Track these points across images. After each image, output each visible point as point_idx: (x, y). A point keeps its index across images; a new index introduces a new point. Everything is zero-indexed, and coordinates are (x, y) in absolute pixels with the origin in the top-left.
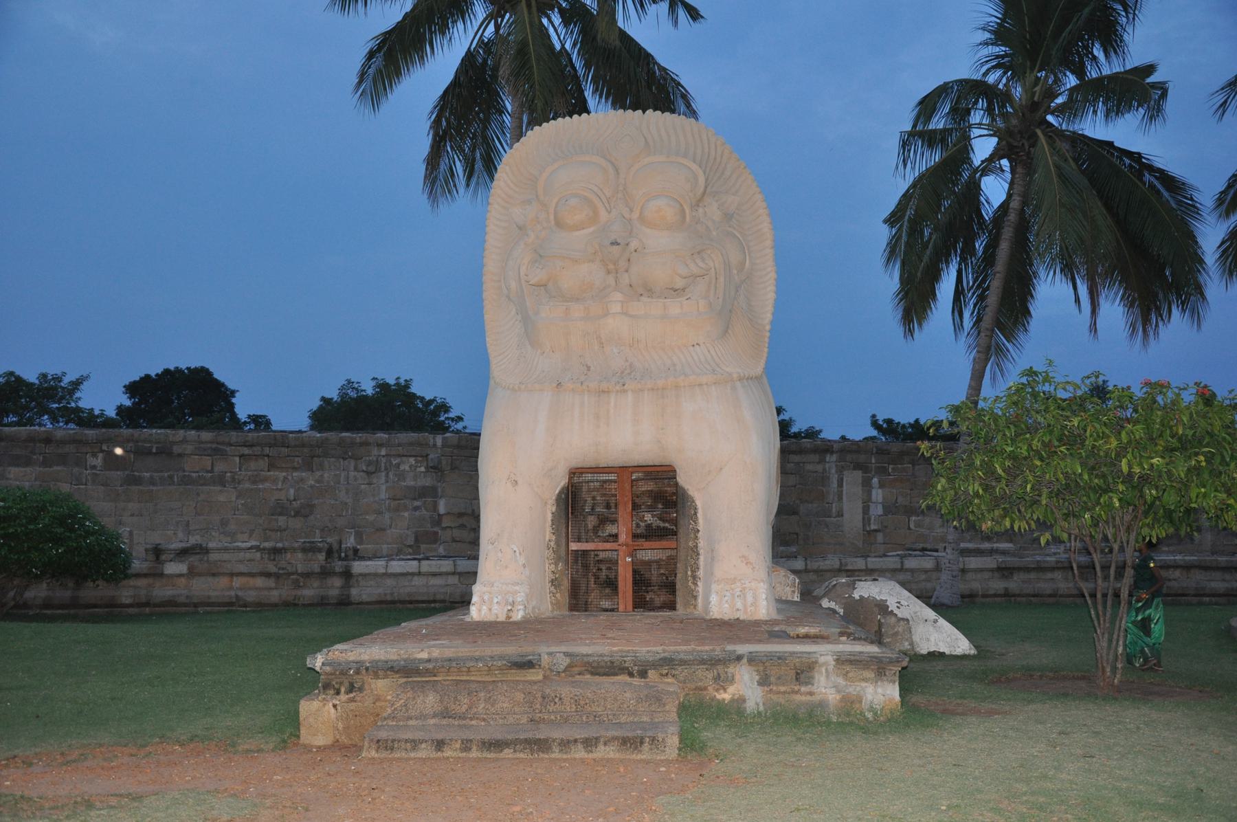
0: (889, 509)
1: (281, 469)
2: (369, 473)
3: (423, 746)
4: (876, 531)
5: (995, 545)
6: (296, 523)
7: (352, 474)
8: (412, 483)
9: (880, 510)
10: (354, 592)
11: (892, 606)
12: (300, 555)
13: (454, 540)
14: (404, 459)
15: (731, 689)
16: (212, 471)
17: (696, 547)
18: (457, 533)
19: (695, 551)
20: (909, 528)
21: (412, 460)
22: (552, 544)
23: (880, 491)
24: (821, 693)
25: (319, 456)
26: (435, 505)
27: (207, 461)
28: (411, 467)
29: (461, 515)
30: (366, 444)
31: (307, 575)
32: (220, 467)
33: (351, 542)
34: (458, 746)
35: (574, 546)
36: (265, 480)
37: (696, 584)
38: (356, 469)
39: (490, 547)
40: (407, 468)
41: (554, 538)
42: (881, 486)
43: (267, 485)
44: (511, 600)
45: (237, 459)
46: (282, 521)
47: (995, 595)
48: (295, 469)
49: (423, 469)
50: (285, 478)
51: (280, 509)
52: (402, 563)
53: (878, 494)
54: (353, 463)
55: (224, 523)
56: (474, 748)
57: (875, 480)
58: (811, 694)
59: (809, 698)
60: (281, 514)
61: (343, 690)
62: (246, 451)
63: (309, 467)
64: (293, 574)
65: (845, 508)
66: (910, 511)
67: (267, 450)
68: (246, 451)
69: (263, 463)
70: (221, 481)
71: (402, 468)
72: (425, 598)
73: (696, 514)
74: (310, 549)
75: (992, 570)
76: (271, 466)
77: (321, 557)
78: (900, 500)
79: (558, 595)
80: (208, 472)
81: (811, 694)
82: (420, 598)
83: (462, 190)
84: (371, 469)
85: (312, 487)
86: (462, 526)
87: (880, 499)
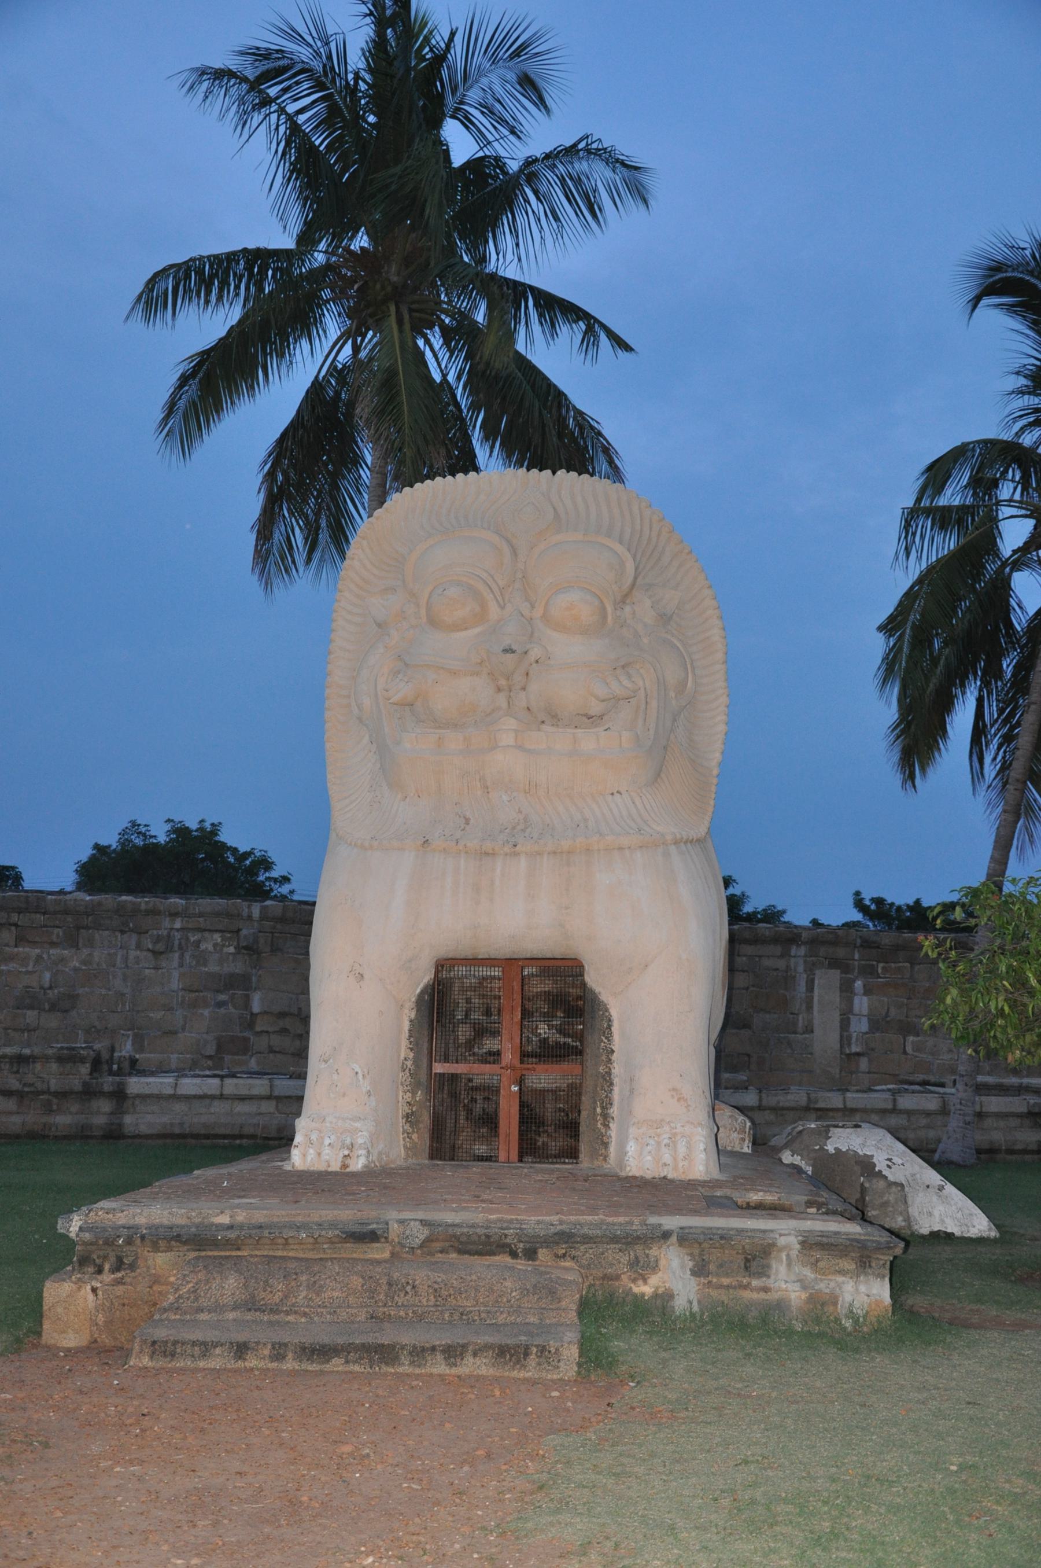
0: (877, 1024)
1: (33, 943)
2: (156, 954)
3: (218, 1351)
4: (858, 1054)
5: (1025, 1081)
6: (52, 1021)
7: (133, 954)
9: (864, 1026)
10: (128, 1119)
11: (881, 1165)
12: (54, 1066)
13: (271, 1050)
14: (207, 934)
15: (654, 1280)
17: (609, 1073)
18: (276, 1041)
19: (607, 1080)
20: (905, 1052)
21: (217, 937)
22: (409, 1063)
23: (865, 999)
24: (780, 1290)
25: (87, 928)
26: (247, 999)
28: (215, 945)
29: (282, 1015)
30: (154, 912)
31: (63, 1095)
33: (126, 1049)
34: (266, 1352)
35: (439, 1068)
36: (12, 958)
37: (607, 1126)
38: (138, 947)
39: (323, 1066)
40: (210, 948)
41: (411, 1055)
42: (868, 991)
43: (12, 966)
44: (348, 1142)
46: (31, 1016)
47: (1025, 1152)
48: (53, 944)
49: (232, 950)
50: (39, 958)
51: (30, 1000)
52: (198, 1081)
53: (862, 1004)
54: (135, 936)
56: (290, 1355)
57: (859, 984)
59: (762, 1295)
60: (31, 1007)
61: (107, 1267)
64: (43, 1093)
65: (816, 1022)
66: (907, 1028)
67: (15, 918)
71: (203, 947)
72: (228, 1132)
73: (609, 1027)
74: (68, 1058)
76: (20, 940)
77: (85, 1069)
78: (893, 1012)
79: (415, 1136)
81: (766, 1290)
82: (222, 1131)
84: (160, 947)
85: (76, 970)
86: (284, 1031)
87: (865, 1011)
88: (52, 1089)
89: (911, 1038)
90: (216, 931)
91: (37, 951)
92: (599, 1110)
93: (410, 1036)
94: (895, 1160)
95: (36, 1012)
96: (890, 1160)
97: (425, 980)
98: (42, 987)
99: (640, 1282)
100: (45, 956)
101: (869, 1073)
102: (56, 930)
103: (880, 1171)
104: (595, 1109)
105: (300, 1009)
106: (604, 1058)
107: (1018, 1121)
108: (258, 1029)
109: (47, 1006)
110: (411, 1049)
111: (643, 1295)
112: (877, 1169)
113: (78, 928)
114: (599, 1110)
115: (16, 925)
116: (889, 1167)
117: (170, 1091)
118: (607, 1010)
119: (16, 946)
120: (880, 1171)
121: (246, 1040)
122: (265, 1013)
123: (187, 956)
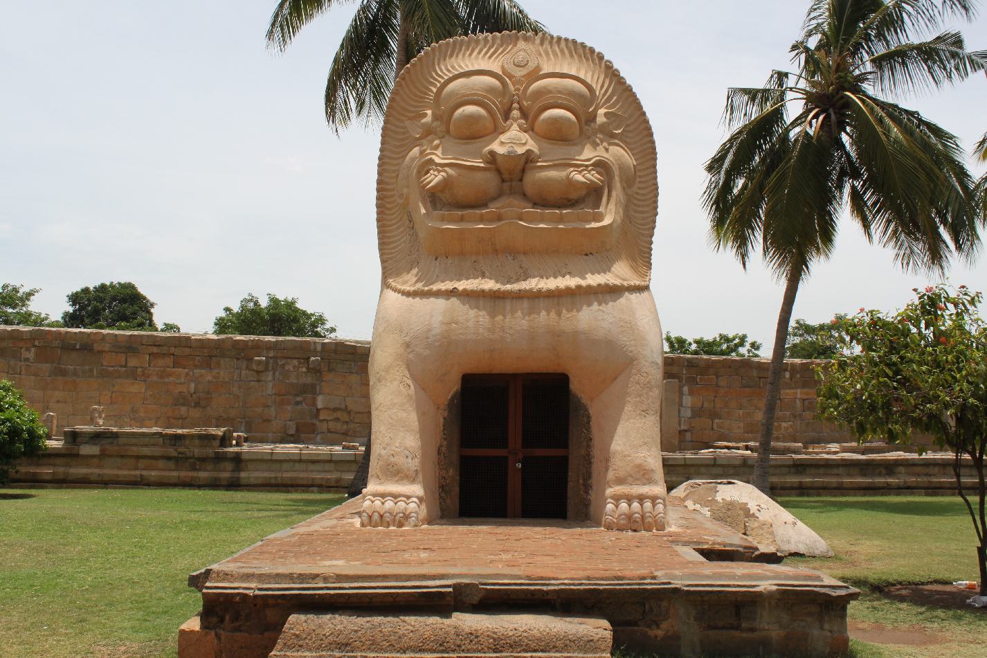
0: (697, 412)
4: (686, 431)
7: (243, 372)
8: (296, 381)
9: (689, 414)
10: (243, 475)
11: (753, 510)
12: (197, 442)
14: (289, 360)
15: (664, 625)
16: (125, 366)
17: (588, 455)
18: (332, 425)
19: (588, 460)
20: (712, 429)
21: (295, 362)
22: (443, 449)
23: (689, 397)
24: (764, 629)
26: (314, 400)
27: (122, 358)
28: (294, 367)
29: (335, 410)
31: (203, 460)
32: (133, 362)
36: (170, 375)
40: (291, 369)
41: (445, 443)
42: (691, 393)
43: (171, 379)
45: (147, 357)
46: (183, 410)
48: (196, 367)
49: (304, 370)
50: (187, 374)
53: (688, 400)
55: (134, 411)
57: (686, 389)
58: (752, 630)
59: (750, 635)
60: (183, 405)
61: (227, 618)
62: (155, 350)
63: (209, 367)
64: (190, 458)
66: (714, 415)
67: (172, 350)
68: (155, 350)
69: (169, 361)
70: (133, 374)
72: (305, 482)
73: (588, 422)
75: (789, 466)
77: (217, 443)
78: (706, 405)
79: (448, 501)
80: (122, 366)
81: (752, 630)
82: (300, 482)
83: (353, 115)
84: (261, 368)
85: (210, 382)
86: (337, 419)
87: (689, 405)
88: (196, 456)
89: (717, 421)
90: (295, 358)
91: (186, 370)
92: (581, 481)
93: (444, 430)
94: (762, 506)
95: (186, 408)
96: (759, 506)
97: (454, 389)
98: (189, 392)
99: (654, 627)
100: (191, 373)
101: (692, 441)
102: (197, 358)
103: (754, 514)
104: (579, 480)
105: (346, 406)
106: (585, 444)
107: (787, 469)
108: (321, 418)
109: (193, 405)
110: (445, 439)
111: (656, 637)
112: (751, 512)
113: (211, 357)
114: (581, 481)
115: (173, 354)
116: (759, 511)
117: (269, 458)
118: (587, 410)
119: (174, 367)
120: (754, 514)
121: (314, 425)
122: (326, 408)
123: (277, 374)
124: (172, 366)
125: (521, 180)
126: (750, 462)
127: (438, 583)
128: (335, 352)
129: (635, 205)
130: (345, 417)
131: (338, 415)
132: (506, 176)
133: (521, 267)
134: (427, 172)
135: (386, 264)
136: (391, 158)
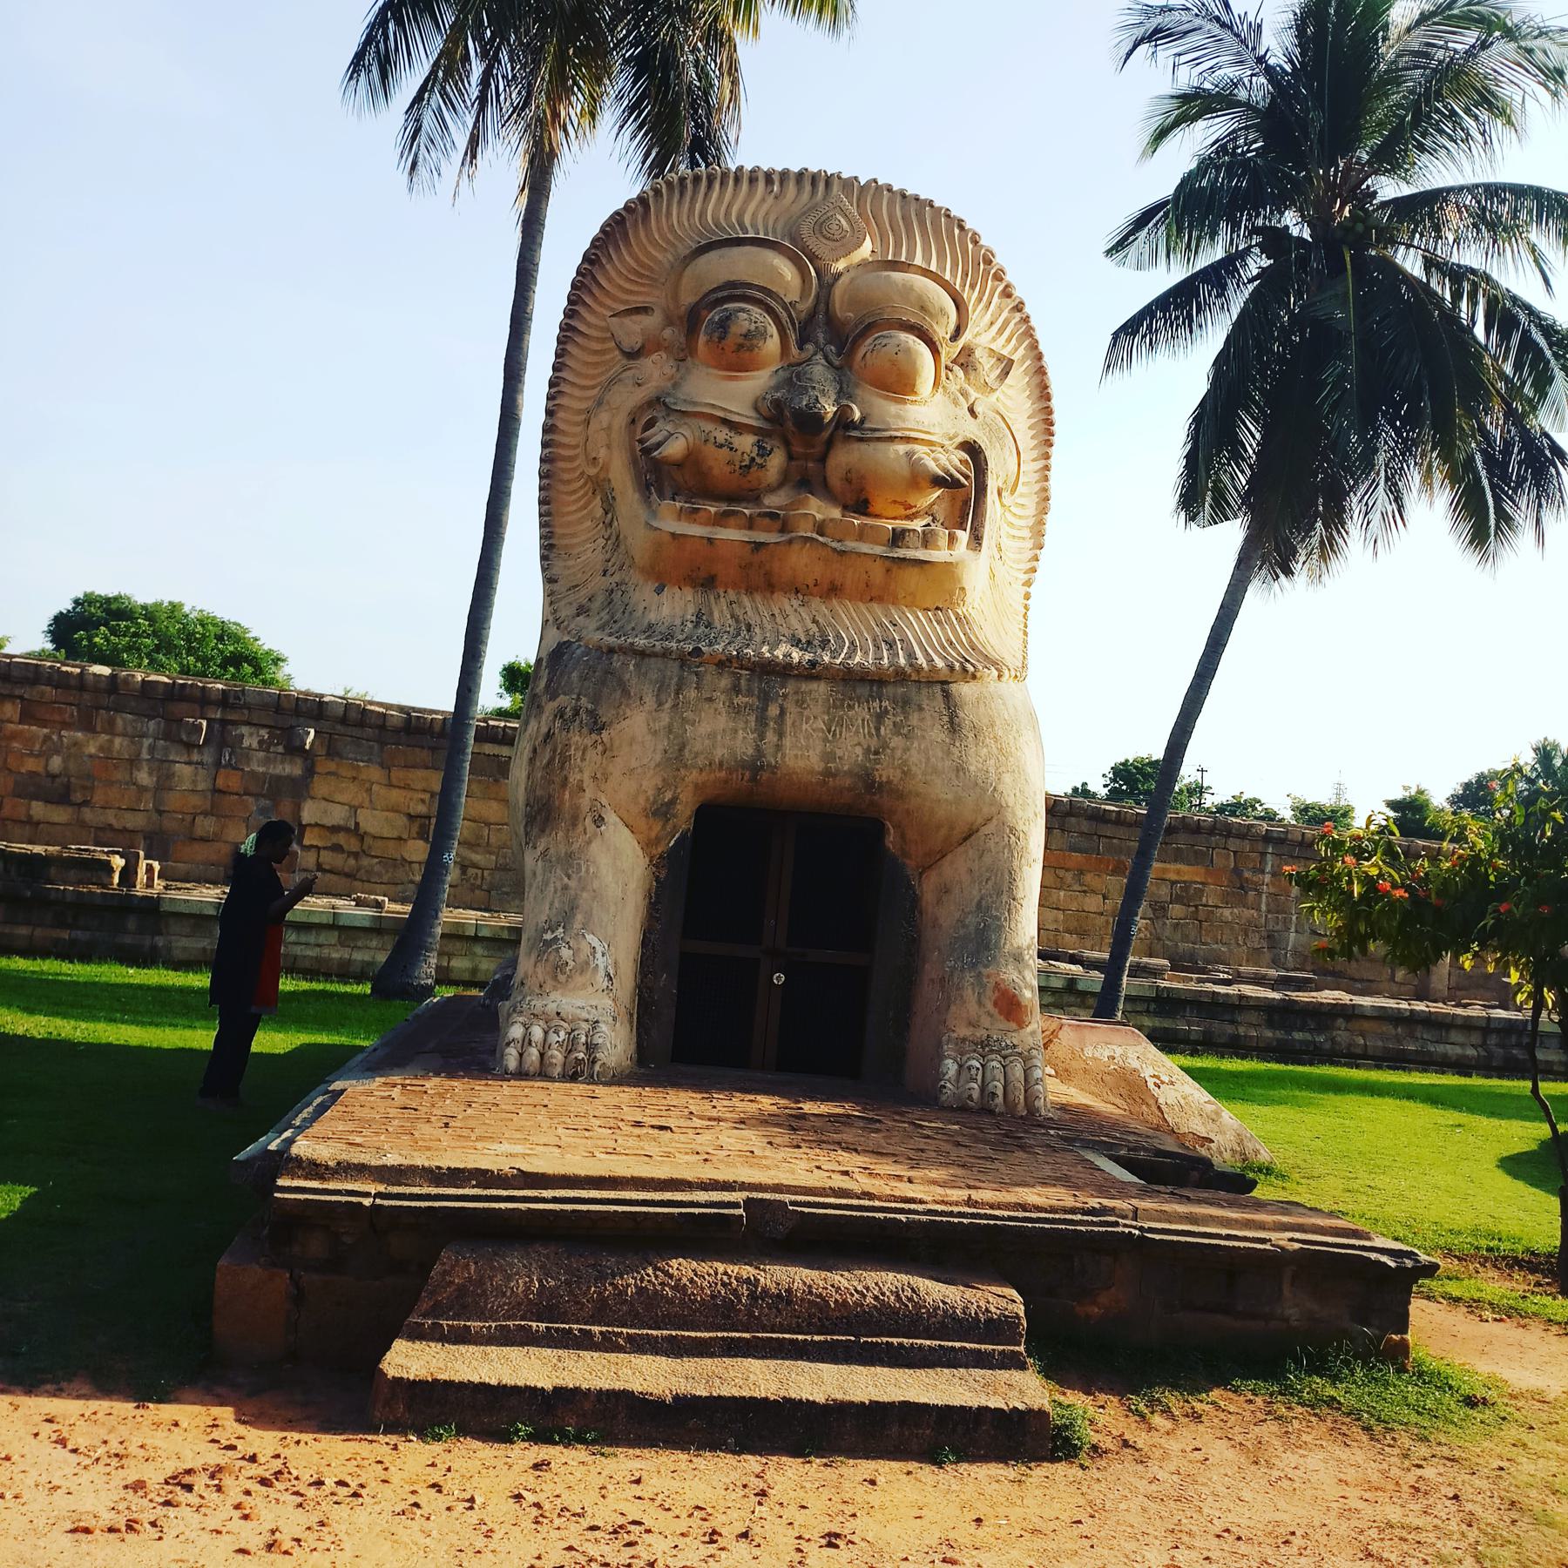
8: (261, 770)
15: (1103, 1299)
18: (327, 858)
29: (335, 829)
48: (66, 725)
49: (280, 749)
50: (47, 738)
63: (89, 728)
86: (337, 848)
90: (264, 726)
91: (46, 731)
100: (55, 737)
105: (357, 824)
108: (306, 842)
119: (20, 723)
122: (317, 825)
124: (16, 717)
125: (823, 459)
126: (1081, 986)
127: (716, 1196)
128: (344, 720)
129: (1010, 524)
130: (352, 844)
131: (341, 839)
132: (798, 449)
133: (814, 621)
134: (650, 424)
135: (555, 587)
136: (573, 384)
